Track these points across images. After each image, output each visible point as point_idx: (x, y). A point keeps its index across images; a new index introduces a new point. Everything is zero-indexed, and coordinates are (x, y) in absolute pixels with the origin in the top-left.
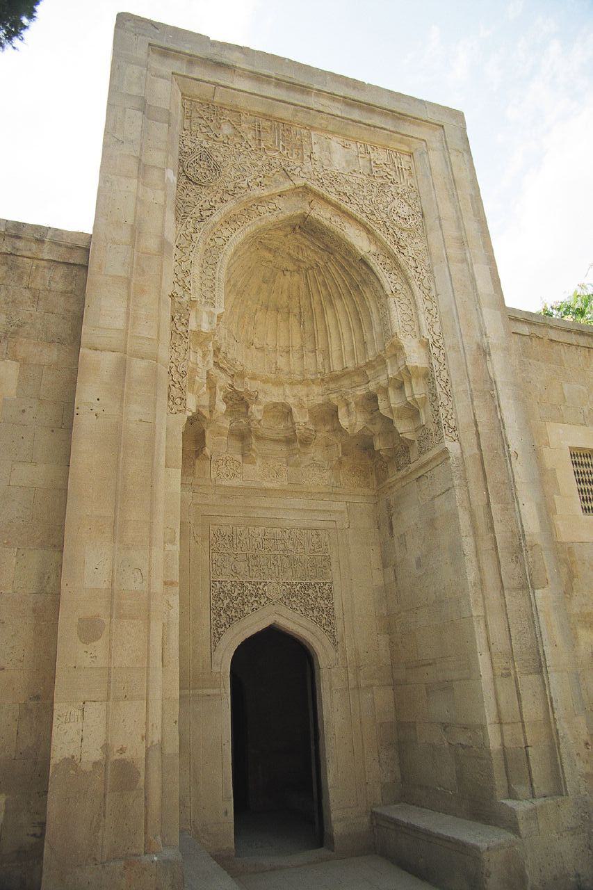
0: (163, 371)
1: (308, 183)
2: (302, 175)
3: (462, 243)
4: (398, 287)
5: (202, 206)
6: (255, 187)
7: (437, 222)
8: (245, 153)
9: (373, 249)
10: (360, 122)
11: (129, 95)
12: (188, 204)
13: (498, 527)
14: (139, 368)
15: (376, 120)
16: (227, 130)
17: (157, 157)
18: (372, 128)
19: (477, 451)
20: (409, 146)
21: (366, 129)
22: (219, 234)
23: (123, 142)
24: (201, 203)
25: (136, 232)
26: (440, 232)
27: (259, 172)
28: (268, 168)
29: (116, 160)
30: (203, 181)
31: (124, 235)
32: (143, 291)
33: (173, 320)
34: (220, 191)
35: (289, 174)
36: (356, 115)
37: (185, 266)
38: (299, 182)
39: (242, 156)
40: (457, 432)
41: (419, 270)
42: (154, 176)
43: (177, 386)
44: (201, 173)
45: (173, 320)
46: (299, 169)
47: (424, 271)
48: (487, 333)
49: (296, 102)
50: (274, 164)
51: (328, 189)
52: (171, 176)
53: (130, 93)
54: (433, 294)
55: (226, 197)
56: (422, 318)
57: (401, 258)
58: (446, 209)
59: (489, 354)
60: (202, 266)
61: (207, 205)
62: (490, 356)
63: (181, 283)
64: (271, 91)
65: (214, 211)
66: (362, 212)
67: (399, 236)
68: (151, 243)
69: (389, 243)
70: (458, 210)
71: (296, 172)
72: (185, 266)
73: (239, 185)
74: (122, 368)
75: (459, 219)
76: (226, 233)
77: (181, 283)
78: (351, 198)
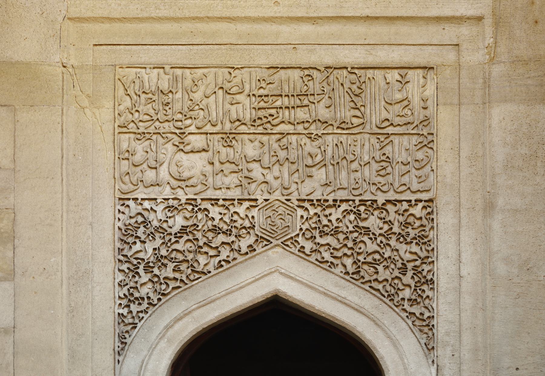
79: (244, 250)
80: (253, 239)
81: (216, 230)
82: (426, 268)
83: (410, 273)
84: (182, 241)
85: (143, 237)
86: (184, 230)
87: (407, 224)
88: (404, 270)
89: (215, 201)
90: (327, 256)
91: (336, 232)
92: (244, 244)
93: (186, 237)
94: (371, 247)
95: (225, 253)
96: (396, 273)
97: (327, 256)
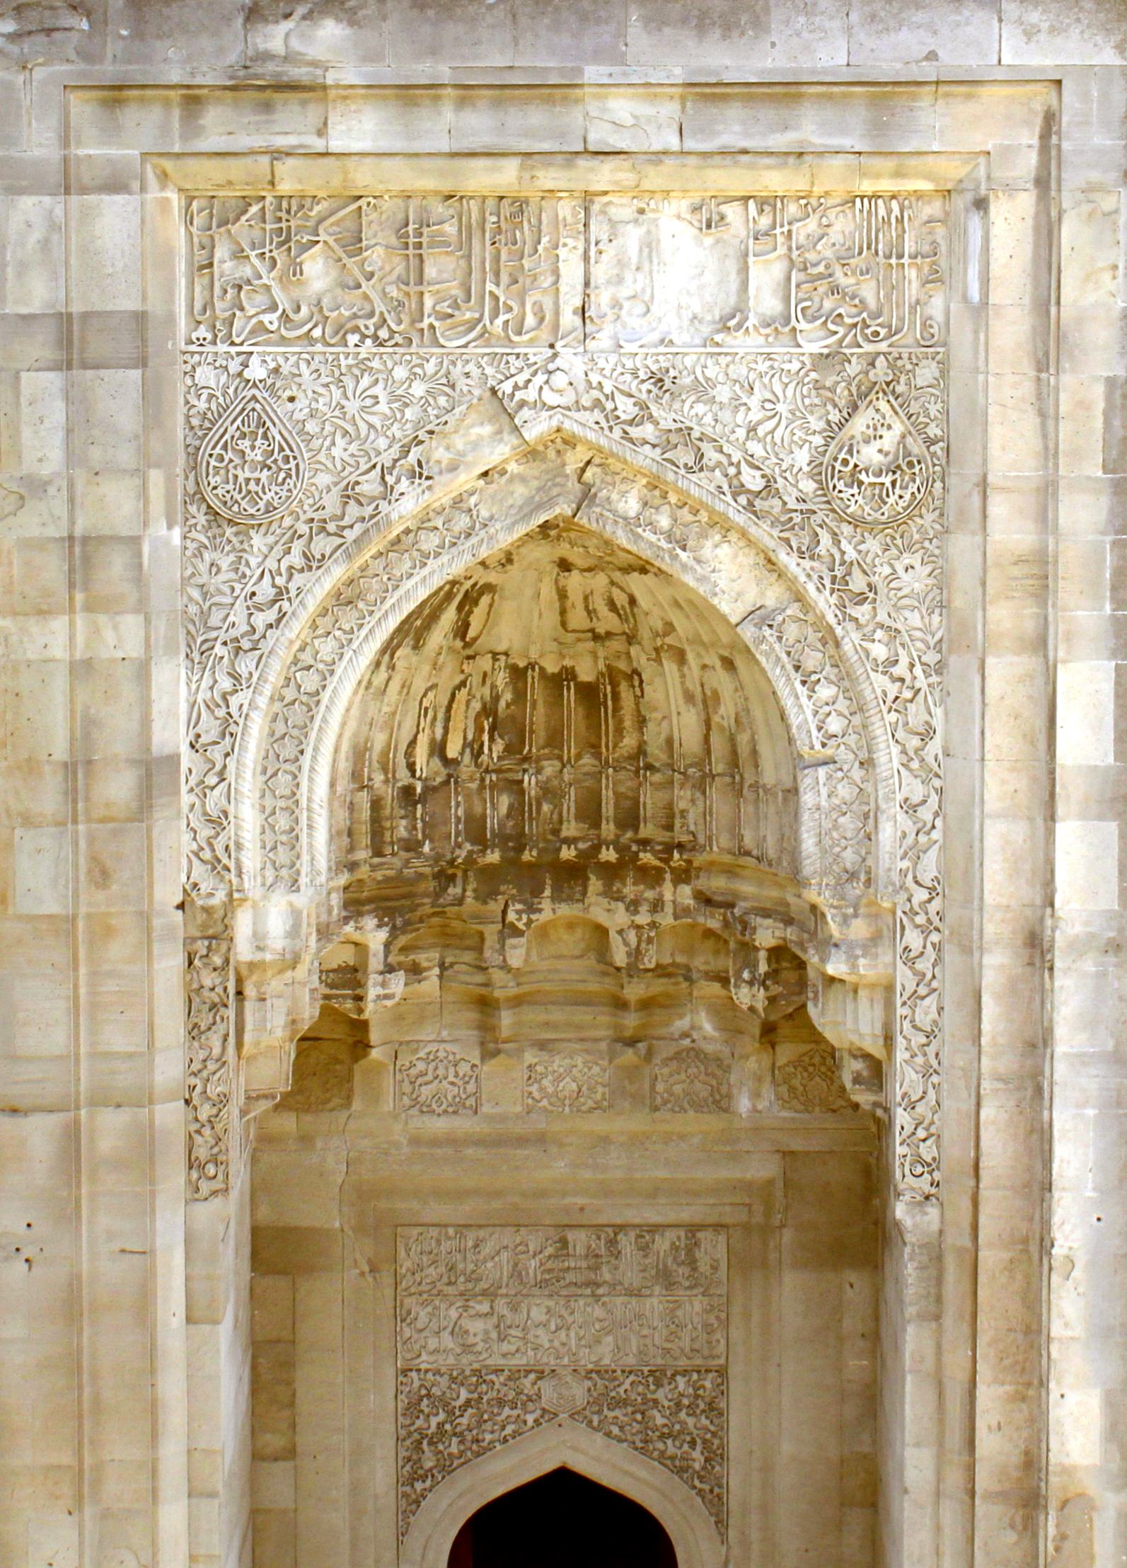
0: (170, 1115)
1: (567, 425)
2: (550, 398)
3: (1040, 575)
4: (834, 725)
5: (254, 594)
6: (404, 484)
7: (976, 500)
8: (376, 364)
9: (773, 595)
10: (745, 152)
11: (24, 317)
12: (217, 599)
13: (987, 1443)
14: (109, 1130)
15: (809, 128)
16: (317, 271)
17: (113, 505)
18: (791, 160)
19: (968, 1243)
20: (927, 177)
21: (769, 167)
22: (307, 658)
23: (22, 498)
24: (249, 589)
25: (79, 769)
26: (979, 539)
27: (418, 425)
28: (442, 401)
29: (10, 564)
30: (252, 511)
31: (49, 800)
32: (110, 932)
33: (190, 963)
34: (303, 528)
35: (511, 406)
36: (732, 128)
37: (215, 800)
38: (536, 428)
39: (366, 381)
40: (937, 1176)
41: (900, 670)
42: (115, 565)
43: (207, 1131)
44: (248, 480)
45: (190, 963)
46: (540, 379)
47: (918, 670)
48: (1057, 904)
49: (525, 146)
50: (462, 384)
51: (634, 432)
52: (166, 539)
53: (24, 310)
54: (935, 747)
55: (322, 545)
56: (887, 834)
57: (851, 640)
58: (1009, 446)
59: (1051, 969)
60: (264, 771)
61: (265, 590)
62: (1051, 977)
63: (207, 855)
64: (442, 126)
65: (286, 604)
66: (735, 496)
67: (851, 554)
68: (118, 788)
69: (811, 588)
70: (1049, 453)
71: (531, 394)
72: (215, 800)
73: (358, 489)
74: (72, 1144)
75: (1047, 494)
76: (326, 648)
77: (207, 855)
78: (706, 447)
79: (530, 1422)
80: (539, 1412)
81: (501, 1403)
82: (716, 1442)
83: (699, 1448)
84: (467, 1414)
85: (426, 1410)
86: (468, 1403)
87: (697, 1397)
88: (693, 1444)
89: (498, 1371)
90: (616, 1430)
91: (624, 1403)
92: (530, 1419)
93: (470, 1411)
94: (660, 1421)
95: (509, 1429)
96: (686, 1447)
97: (616, 1430)
